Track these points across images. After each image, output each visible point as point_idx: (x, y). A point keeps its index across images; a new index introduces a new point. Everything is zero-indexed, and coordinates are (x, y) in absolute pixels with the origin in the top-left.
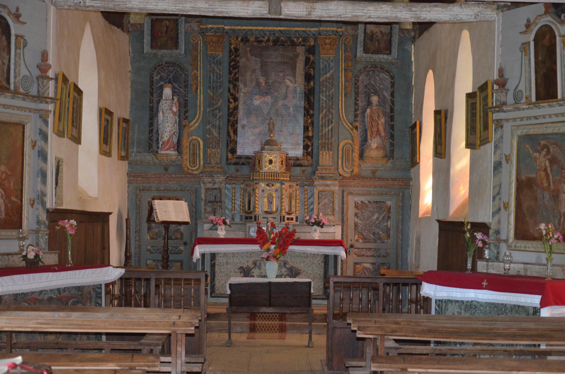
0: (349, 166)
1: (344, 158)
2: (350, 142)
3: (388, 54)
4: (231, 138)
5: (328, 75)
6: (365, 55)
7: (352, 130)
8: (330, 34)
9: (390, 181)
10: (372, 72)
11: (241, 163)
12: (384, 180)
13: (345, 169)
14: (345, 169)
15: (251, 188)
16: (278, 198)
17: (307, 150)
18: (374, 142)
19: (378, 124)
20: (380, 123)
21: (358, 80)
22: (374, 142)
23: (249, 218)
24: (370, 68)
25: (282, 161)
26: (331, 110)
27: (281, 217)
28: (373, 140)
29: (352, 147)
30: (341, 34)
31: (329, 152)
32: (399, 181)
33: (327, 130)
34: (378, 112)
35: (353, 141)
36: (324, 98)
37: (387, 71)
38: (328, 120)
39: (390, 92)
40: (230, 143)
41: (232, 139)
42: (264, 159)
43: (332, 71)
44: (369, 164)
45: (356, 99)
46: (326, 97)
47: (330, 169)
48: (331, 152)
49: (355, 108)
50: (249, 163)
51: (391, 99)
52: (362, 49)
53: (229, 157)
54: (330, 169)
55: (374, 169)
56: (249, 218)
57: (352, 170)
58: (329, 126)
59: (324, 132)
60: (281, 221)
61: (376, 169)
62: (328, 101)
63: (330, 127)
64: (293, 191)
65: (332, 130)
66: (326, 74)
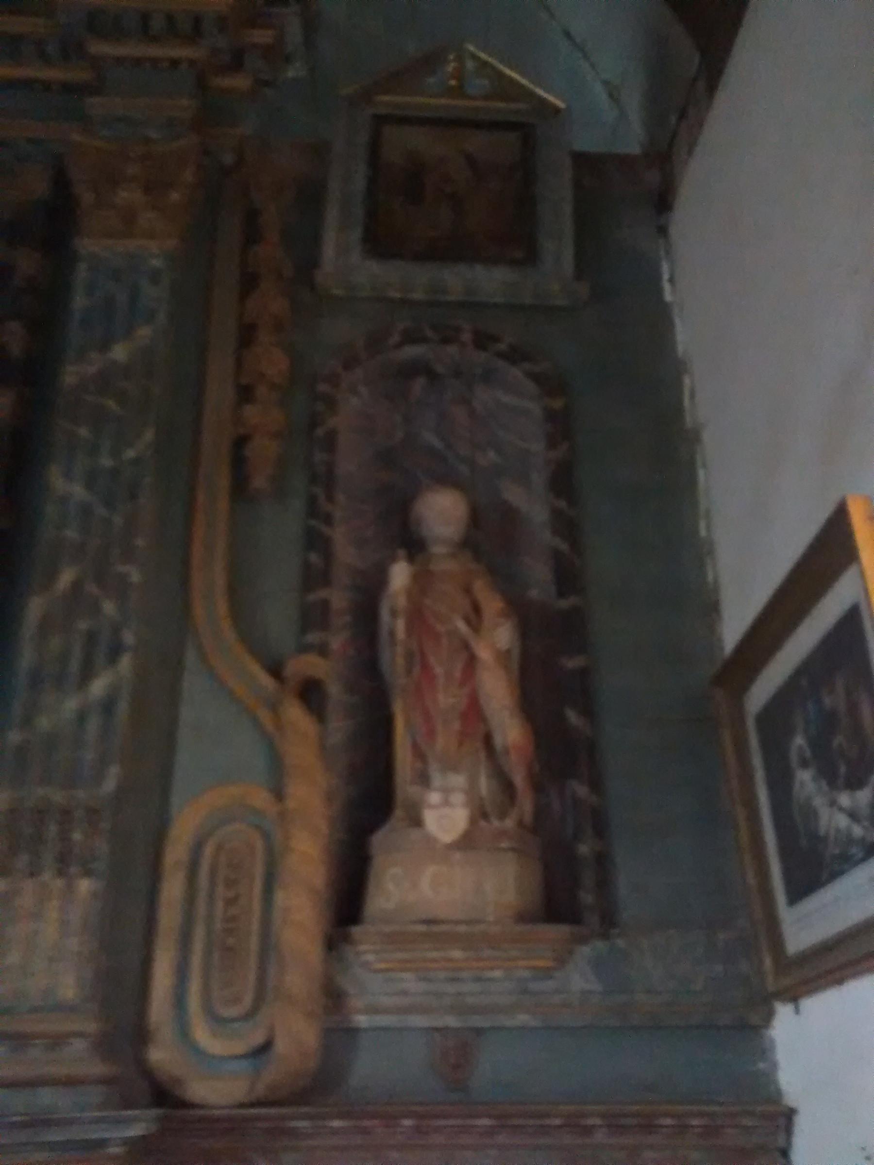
0: (237, 1000)
1: (199, 933)
2: (261, 799)
3: (514, 263)
5: (119, 353)
6: (374, 267)
7: (274, 707)
8: (153, 134)
9: (600, 1137)
10: (418, 385)
12: (544, 1130)
13: (202, 1035)
14: (202, 1035)
18: (446, 791)
19: (472, 661)
20: (484, 654)
21: (331, 404)
22: (446, 791)
24: (411, 337)
26: (122, 569)
28: (437, 779)
29: (266, 836)
30: (228, 159)
31: (70, 888)
32: (682, 1129)
33: (71, 705)
34: (468, 590)
35: (279, 795)
36: (78, 491)
37: (515, 356)
38: (91, 638)
39: (539, 479)
43: (144, 332)
44: (409, 981)
45: (312, 509)
46: (90, 484)
47: (57, 1041)
48: (85, 886)
49: (307, 566)
51: (556, 513)
52: (357, 234)
54: (57, 1041)
55: (451, 1021)
57: (258, 1038)
58: (87, 674)
59: (44, 723)
61: (478, 1021)
62: (101, 511)
63: (98, 687)
65: (108, 706)
66: (105, 346)
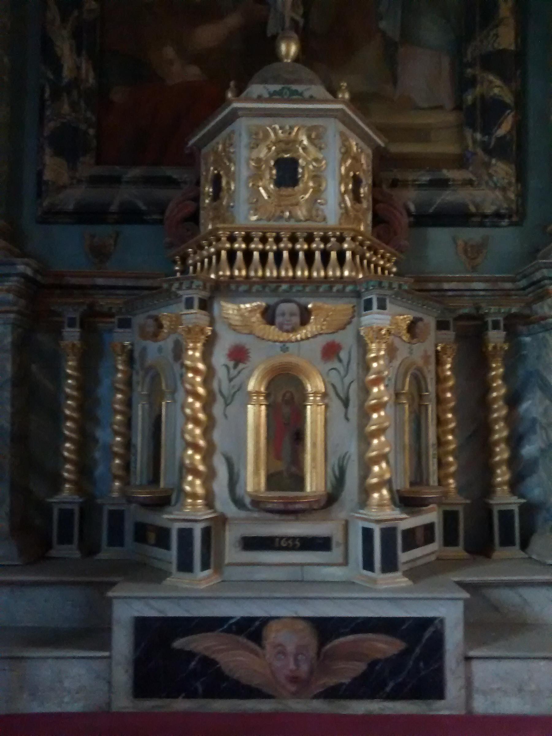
4: (57, 68)
11: (113, 208)
15: (168, 344)
16: (346, 403)
17: (487, 130)
23: (152, 537)
25: (357, 182)
27: (368, 534)
40: (56, 95)
41: (67, 73)
42: (243, 153)
50: (161, 207)
53: (48, 176)
56: (152, 537)
60: (368, 564)
64: (426, 358)
